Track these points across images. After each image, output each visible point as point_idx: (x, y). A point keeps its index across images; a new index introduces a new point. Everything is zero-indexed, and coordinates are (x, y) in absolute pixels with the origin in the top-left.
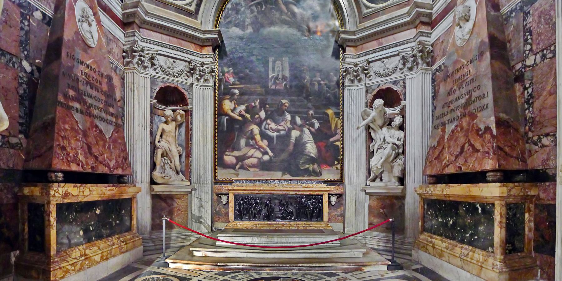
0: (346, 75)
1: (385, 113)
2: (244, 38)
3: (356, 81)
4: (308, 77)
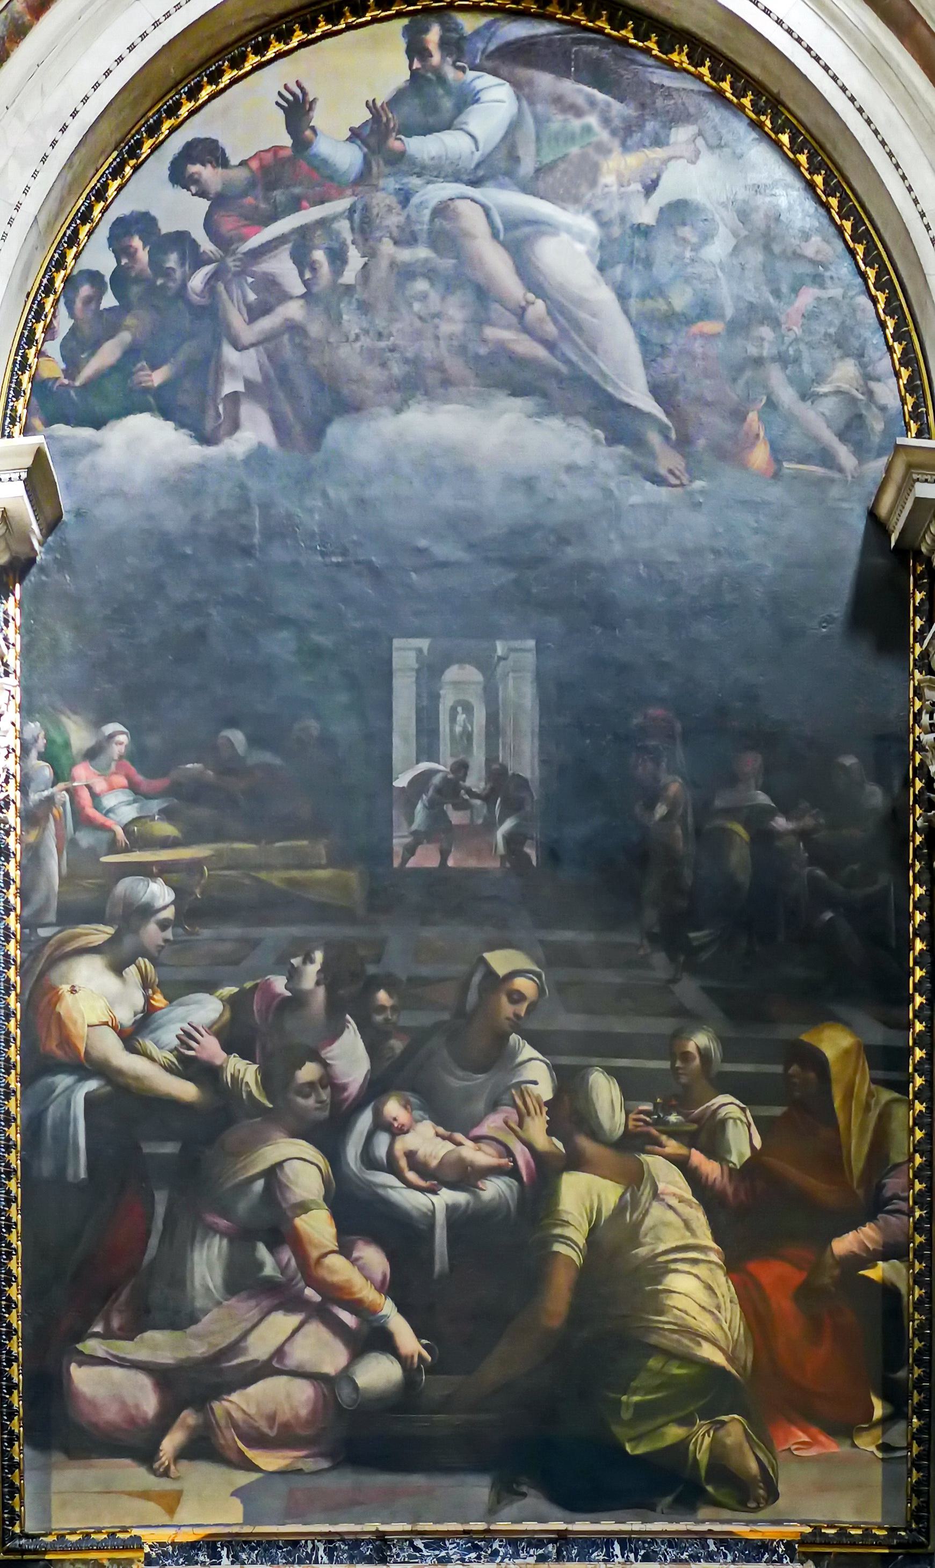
4: (675, 787)
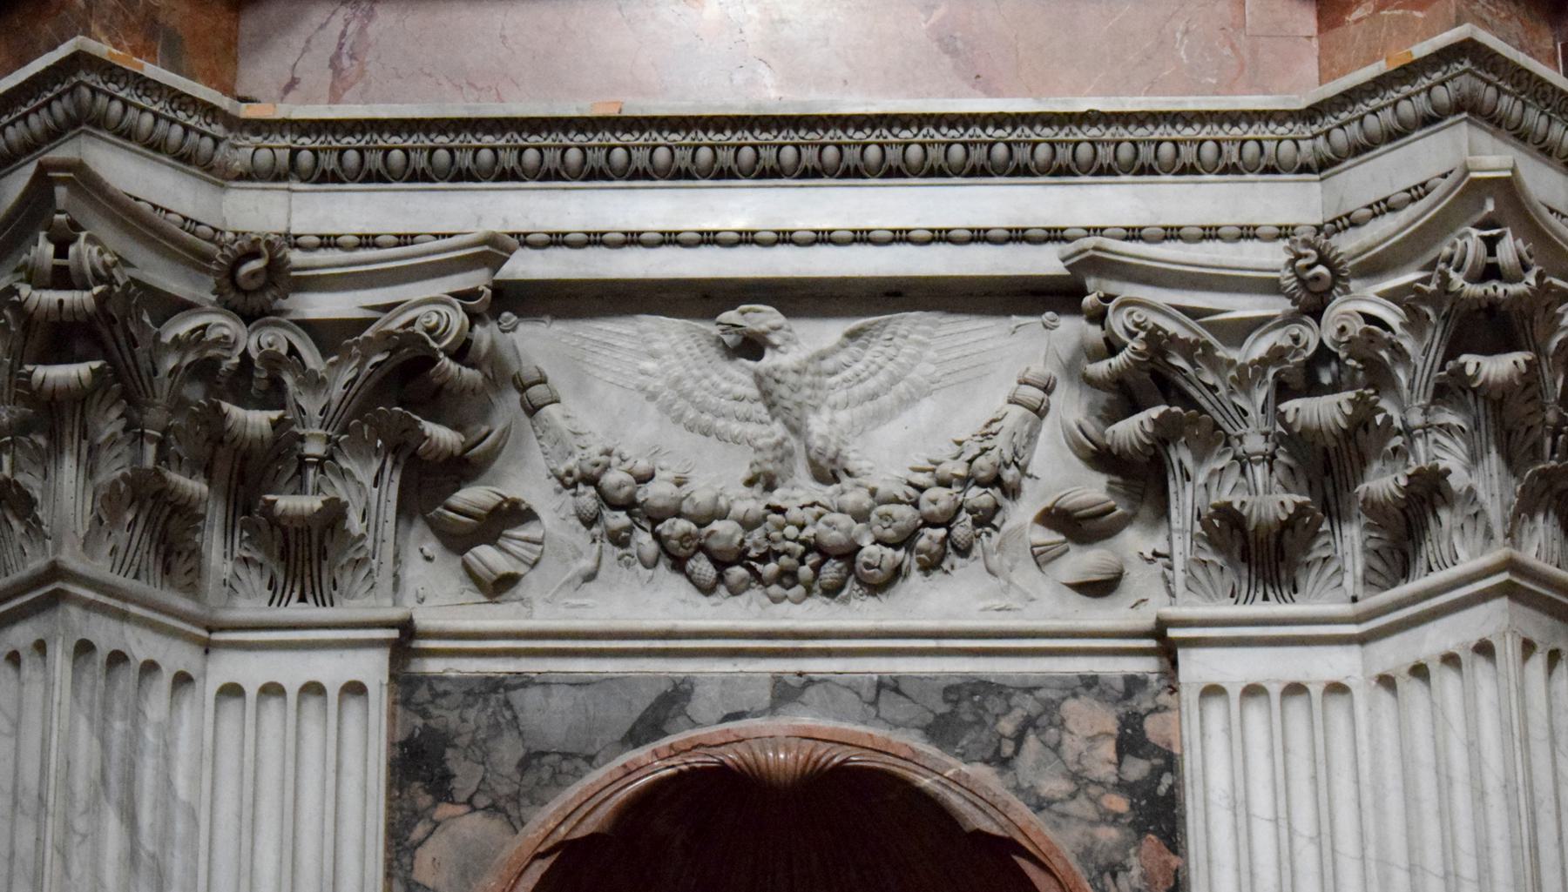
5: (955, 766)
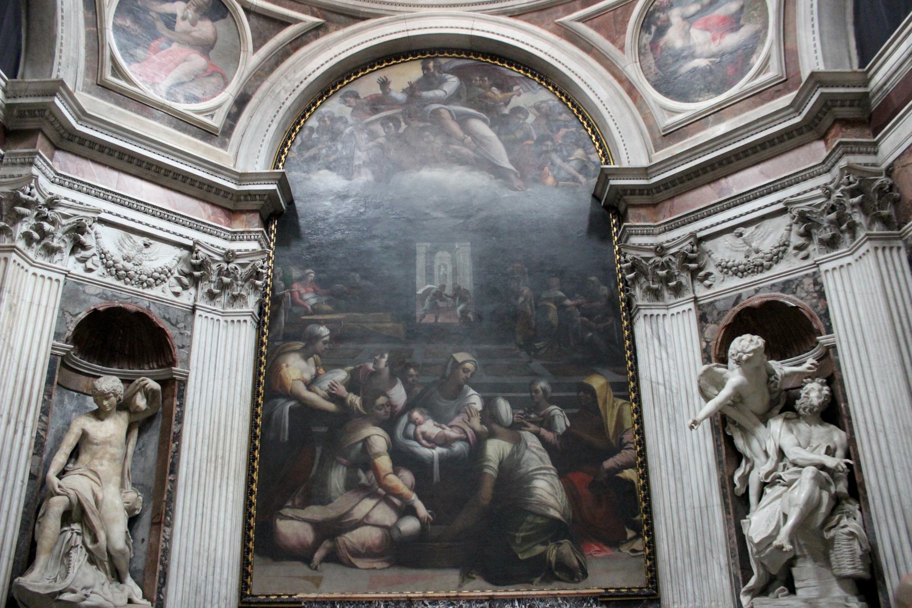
0: (634, 280)
1: (771, 373)
2: (351, 197)
3: (666, 294)
5: (786, 296)
